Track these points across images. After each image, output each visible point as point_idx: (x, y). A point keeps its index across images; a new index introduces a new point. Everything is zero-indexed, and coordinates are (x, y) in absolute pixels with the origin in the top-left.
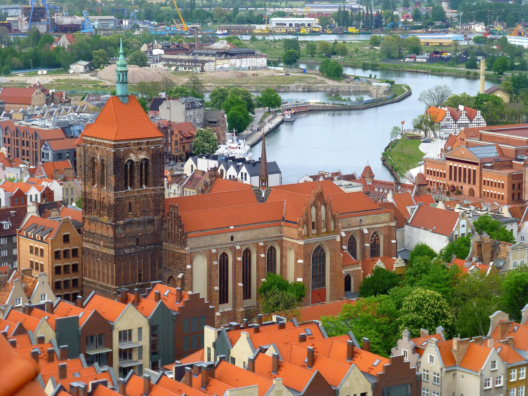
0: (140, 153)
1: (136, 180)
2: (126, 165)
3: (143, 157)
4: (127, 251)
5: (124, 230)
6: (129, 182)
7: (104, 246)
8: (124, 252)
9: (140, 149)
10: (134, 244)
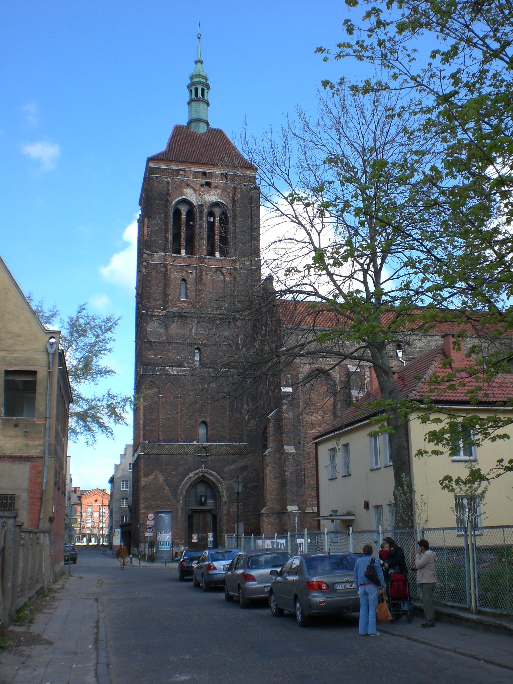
0: (208, 192)
1: (202, 245)
5: (167, 327)
6: (183, 244)
8: (163, 370)
9: (208, 184)
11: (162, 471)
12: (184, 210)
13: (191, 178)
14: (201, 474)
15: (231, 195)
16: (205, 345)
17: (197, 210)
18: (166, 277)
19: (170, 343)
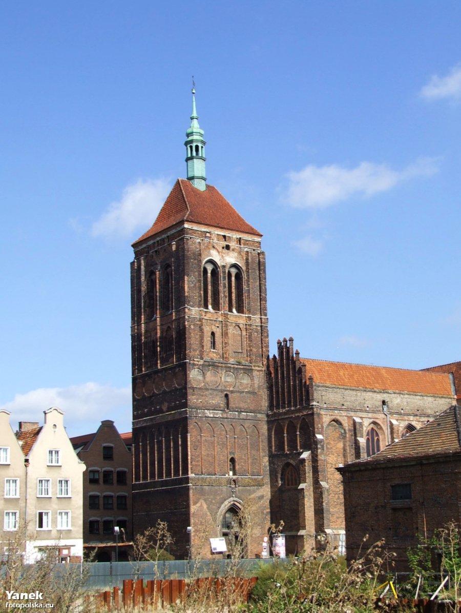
2: (205, 270)
3: (233, 261)
4: (209, 413)
5: (204, 375)
7: (169, 409)
9: (228, 247)
10: (222, 404)
11: (205, 500)
12: (210, 268)
13: (215, 241)
14: (232, 503)
15: (245, 258)
16: (232, 392)
17: (220, 270)
18: (201, 330)
19: (207, 389)
